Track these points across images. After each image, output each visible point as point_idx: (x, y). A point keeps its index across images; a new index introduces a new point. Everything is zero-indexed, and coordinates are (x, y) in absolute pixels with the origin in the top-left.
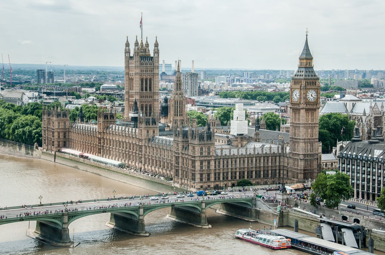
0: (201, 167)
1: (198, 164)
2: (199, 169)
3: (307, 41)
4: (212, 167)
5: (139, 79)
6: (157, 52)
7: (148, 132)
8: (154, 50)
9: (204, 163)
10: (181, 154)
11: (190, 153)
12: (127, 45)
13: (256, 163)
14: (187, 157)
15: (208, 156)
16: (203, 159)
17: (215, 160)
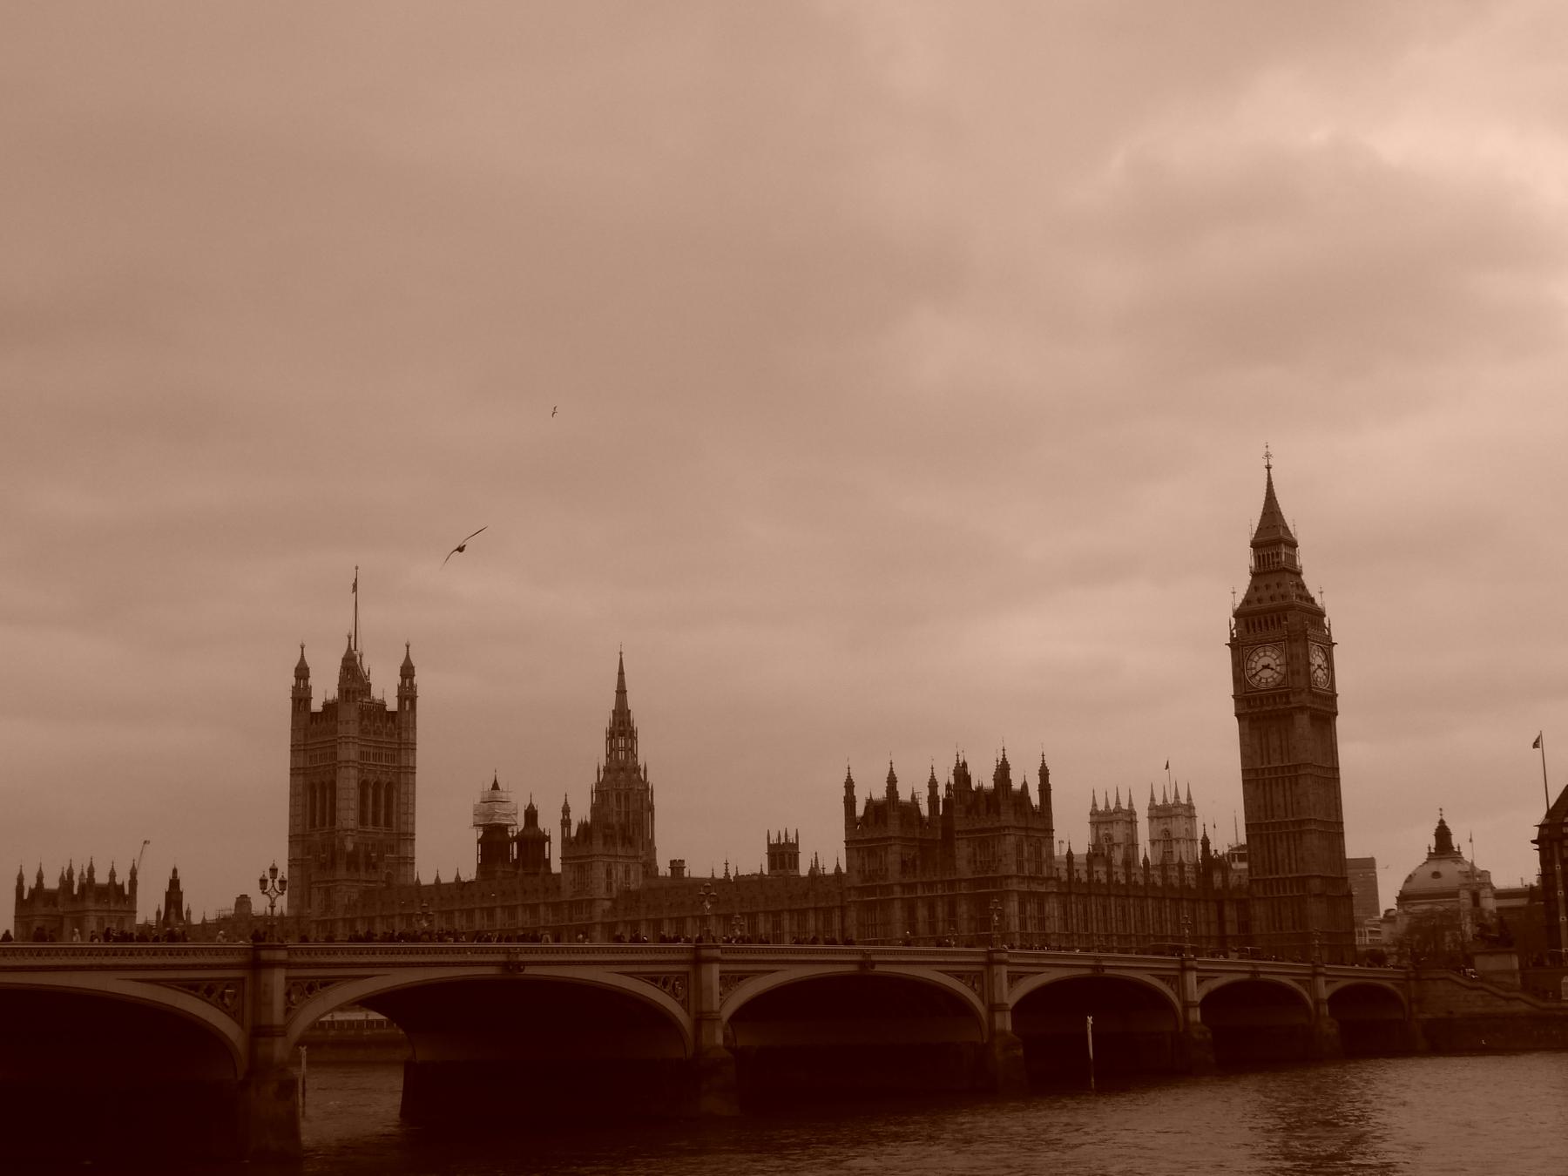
0: (1023, 924)
1: (1013, 907)
2: (1017, 929)
3: (1270, 484)
4: (1054, 925)
5: (354, 783)
6: (407, 694)
7: (609, 873)
8: (401, 688)
9: (1028, 908)
10: (897, 889)
11: (964, 869)
12: (302, 672)
13: (1153, 924)
14: (940, 892)
15: (1038, 878)
16: (1024, 888)
17: (1058, 894)
